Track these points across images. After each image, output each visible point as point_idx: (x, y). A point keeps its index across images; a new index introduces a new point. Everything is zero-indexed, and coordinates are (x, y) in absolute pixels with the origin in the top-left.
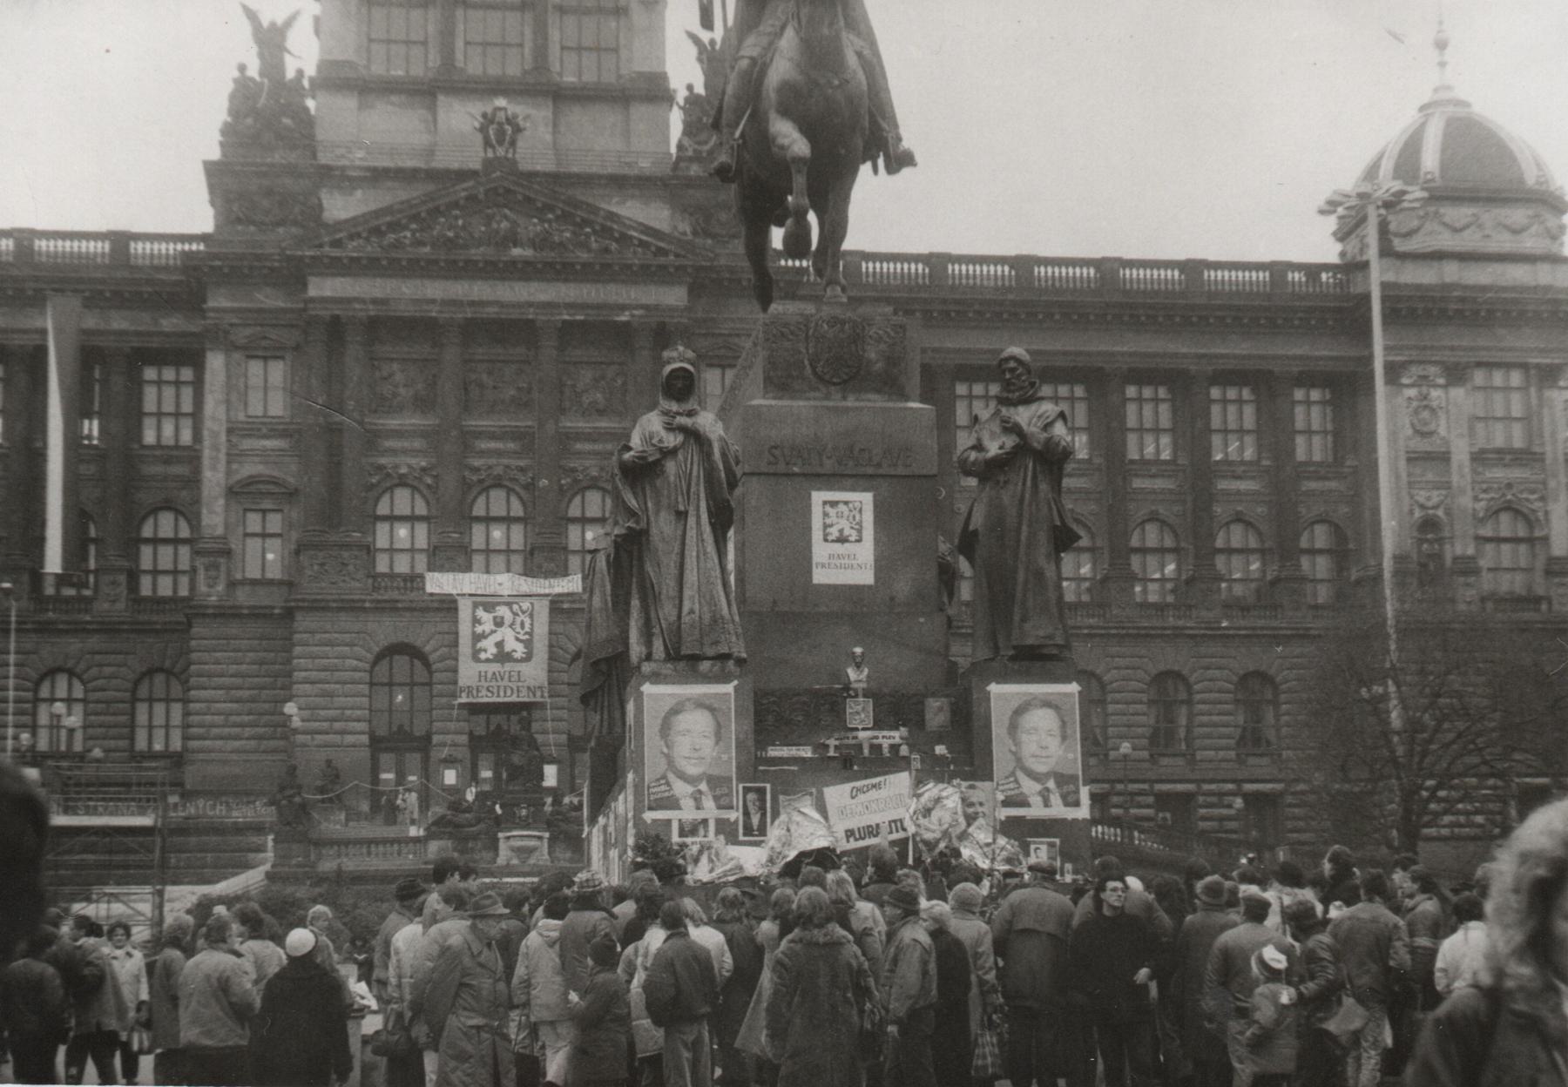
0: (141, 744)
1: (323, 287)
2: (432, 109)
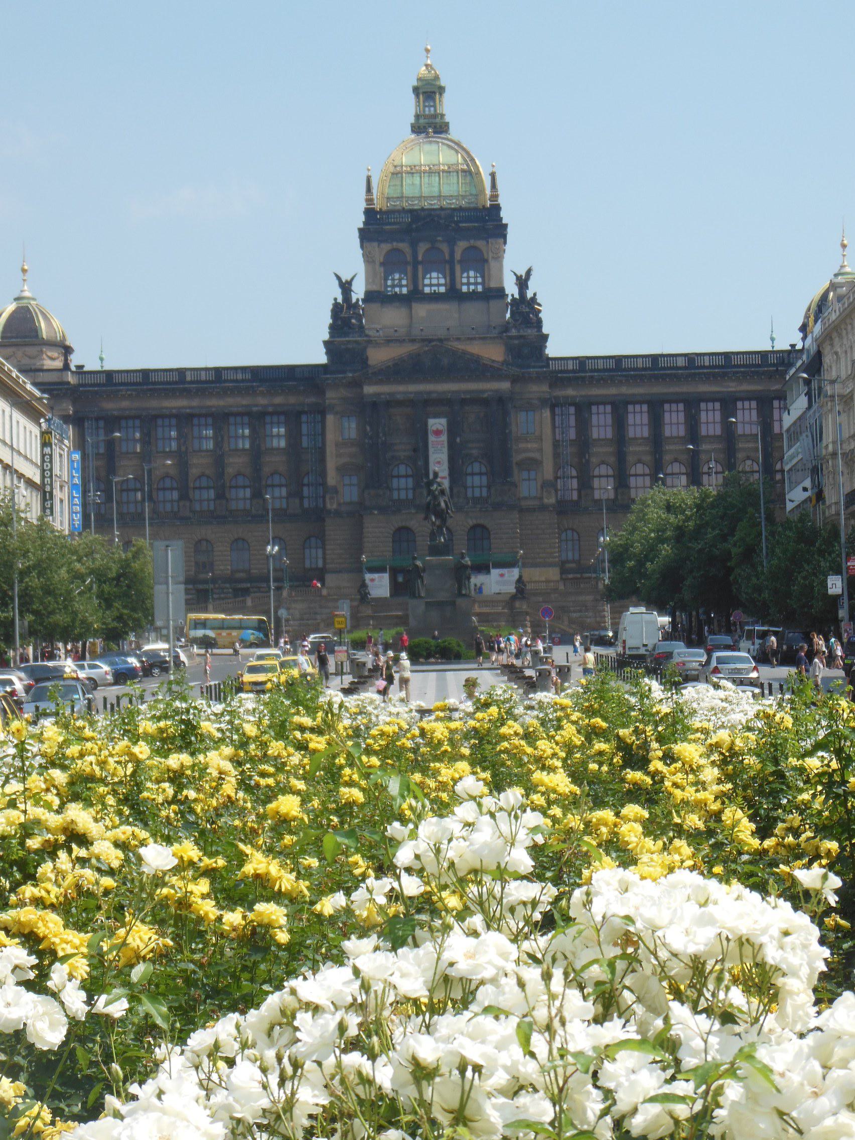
0: (307, 565)
1: (369, 390)
2: (411, 308)
